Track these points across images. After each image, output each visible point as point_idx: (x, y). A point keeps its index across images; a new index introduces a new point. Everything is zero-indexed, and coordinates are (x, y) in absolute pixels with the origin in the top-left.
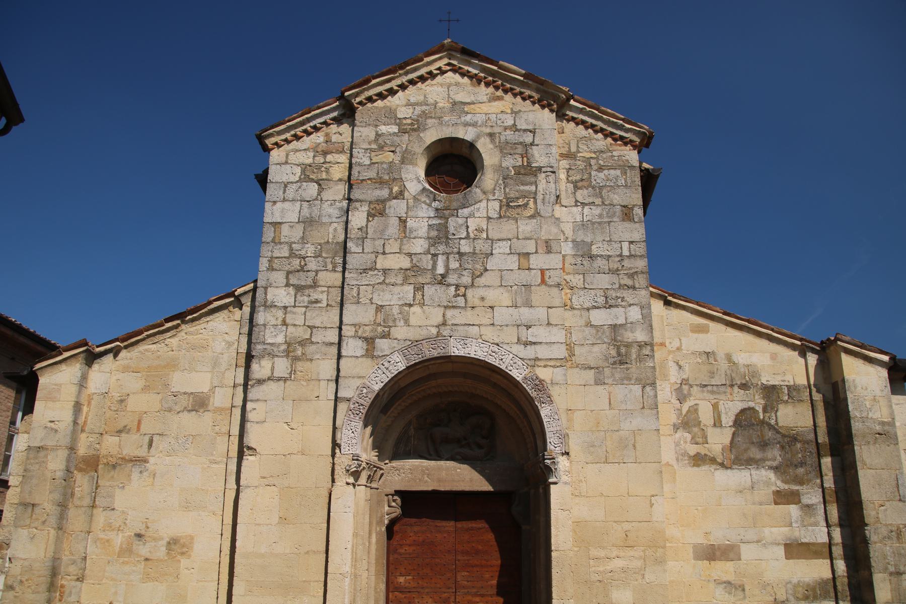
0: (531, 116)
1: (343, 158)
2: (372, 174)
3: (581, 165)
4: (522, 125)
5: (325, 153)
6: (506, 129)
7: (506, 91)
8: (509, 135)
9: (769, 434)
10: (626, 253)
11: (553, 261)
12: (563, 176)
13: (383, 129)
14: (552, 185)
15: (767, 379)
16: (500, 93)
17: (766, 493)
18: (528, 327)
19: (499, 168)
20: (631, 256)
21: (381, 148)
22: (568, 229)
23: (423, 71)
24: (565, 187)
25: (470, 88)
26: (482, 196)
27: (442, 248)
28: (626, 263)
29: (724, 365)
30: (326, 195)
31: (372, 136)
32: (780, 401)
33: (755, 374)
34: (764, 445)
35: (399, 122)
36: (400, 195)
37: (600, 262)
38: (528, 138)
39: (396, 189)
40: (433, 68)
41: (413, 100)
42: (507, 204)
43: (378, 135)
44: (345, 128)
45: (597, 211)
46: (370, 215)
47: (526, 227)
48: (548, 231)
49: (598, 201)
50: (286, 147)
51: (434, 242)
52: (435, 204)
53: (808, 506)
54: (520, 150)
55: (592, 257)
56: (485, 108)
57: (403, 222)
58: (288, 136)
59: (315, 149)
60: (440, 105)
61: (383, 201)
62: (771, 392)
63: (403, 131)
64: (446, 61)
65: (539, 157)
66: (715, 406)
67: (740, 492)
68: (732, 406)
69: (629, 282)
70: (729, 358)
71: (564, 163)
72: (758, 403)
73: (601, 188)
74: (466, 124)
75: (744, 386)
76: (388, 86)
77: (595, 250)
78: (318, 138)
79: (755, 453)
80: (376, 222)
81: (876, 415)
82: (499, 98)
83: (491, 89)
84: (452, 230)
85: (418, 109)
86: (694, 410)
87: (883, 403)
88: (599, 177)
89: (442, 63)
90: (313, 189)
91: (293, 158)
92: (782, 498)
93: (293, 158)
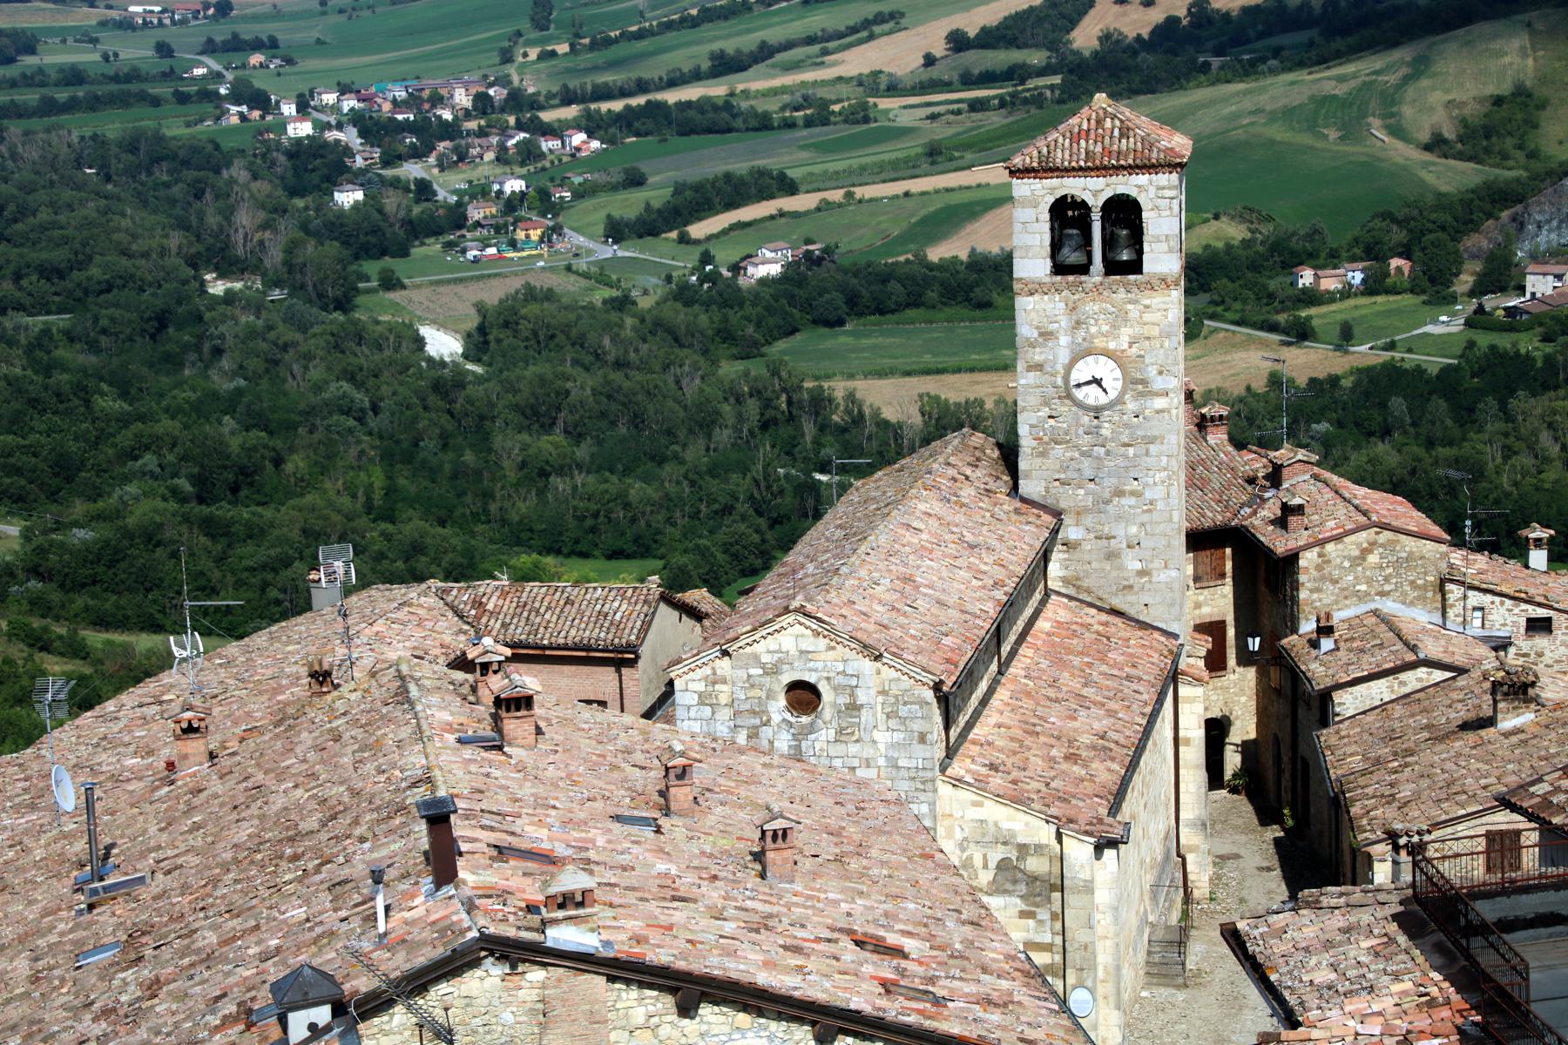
0: (856, 664)
2: (748, 707)
3: (892, 700)
4: (850, 672)
5: (714, 683)
8: (841, 680)
9: (1019, 875)
12: (879, 708)
13: (754, 671)
15: (1021, 839)
17: (1014, 911)
19: (834, 705)
21: (752, 686)
22: (882, 747)
29: (992, 828)
30: (717, 716)
32: (1027, 854)
33: (1014, 835)
34: (1015, 882)
35: (763, 666)
36: (767, 723)
37: (903, 773)
38: (854, 682)
40: (784, 624)
42: (840, 731)
43: (749, 676)
45: (902, 735)
46: (749, 737)
47: (853, 749)
48: (868, 752)
50: (686, 677)
53: (1041, 922)
55: (898, 768)
56: (823, 656)
59: (706, 678)
61: (756, 727)
62: (1023, 849)
63: (766, 673)
65: (862, 697)
66: (985, 856)
68: (996, 855)
69: (920, 786)
70: (996, 824)
71: (880, 699)
72: (1013, 855)
74: (811, 670)
75: (1005, 843)
77: (900, 763)
78: (707, 671)
79: (1009, 886)
81: (1081, 876)
82: (833, 648)
85: (776, 657)
86: (970, 858)
87: (1087, 868)
88: (903, 711)
90: (707, 711)
91: (691, 686)
92: (1024, 915)
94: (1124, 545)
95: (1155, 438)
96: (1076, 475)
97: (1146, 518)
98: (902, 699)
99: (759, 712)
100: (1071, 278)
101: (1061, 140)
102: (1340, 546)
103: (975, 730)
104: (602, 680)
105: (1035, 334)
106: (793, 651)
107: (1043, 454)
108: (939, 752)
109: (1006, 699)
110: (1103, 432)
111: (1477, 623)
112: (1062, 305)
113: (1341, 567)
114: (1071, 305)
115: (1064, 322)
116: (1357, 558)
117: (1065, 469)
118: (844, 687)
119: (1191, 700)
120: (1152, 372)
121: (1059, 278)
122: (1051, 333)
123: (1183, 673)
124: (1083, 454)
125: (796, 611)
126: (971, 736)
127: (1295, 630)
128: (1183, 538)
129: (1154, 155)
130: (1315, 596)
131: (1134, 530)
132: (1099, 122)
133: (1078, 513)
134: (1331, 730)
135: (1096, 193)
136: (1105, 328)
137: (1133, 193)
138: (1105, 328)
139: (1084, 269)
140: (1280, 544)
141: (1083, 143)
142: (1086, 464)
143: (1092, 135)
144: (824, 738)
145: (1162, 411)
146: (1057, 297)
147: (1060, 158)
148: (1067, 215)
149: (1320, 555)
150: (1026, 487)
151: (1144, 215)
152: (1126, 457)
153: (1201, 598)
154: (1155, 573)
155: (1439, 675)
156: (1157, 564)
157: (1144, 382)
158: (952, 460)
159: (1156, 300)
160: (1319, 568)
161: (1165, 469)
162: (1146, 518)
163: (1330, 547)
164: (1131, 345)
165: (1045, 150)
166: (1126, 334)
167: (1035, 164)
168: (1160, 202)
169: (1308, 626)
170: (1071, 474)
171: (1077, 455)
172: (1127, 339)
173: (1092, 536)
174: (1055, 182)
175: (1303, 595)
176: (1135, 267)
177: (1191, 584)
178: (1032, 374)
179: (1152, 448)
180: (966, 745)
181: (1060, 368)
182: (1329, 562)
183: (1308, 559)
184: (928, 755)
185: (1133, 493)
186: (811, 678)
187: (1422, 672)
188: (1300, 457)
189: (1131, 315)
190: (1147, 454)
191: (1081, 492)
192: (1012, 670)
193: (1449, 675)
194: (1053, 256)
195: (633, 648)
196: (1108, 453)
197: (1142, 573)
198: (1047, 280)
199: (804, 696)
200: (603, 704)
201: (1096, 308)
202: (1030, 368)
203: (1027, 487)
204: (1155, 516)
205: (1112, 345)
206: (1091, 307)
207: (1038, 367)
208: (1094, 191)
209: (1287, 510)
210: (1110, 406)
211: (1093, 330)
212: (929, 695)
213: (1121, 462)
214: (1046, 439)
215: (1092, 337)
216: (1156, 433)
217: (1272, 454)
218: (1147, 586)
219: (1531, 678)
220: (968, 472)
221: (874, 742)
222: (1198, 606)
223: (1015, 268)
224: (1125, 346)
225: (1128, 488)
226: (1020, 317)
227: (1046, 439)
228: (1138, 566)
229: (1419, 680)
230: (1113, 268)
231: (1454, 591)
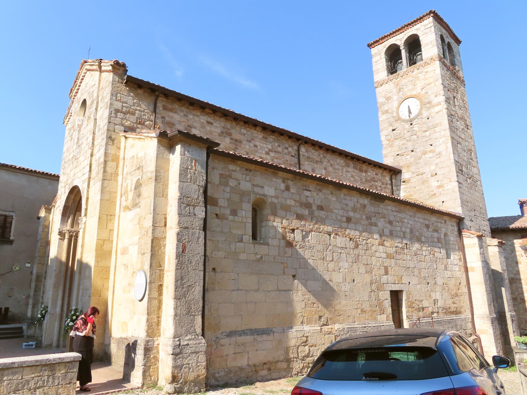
18: (85, 168)
23: (81, 77)
40: (83, 74)
67: (132, 221)
89: (84, 71)
94: (429, 176)
95: (437, 124)
97: (438, 161)
105: (384, 99)
107: (391, 146)
110: (415, 129)
112: (393, 85)
114: (396, 83)
115: (395, 91)
117: (400, 149)
120: (432, 97)
122: (390, 97)
124: (407, 141)
131: (433, 167)
133: (408, 166)
136: (411, 87)
137: (415, 32)
138: (411, 87)
145: (439, 112)
146: (391, 83)
151: (420, 38)
152: (426, 136)
157: (429, 102)
159: (429, 68)
161: (444, 136)
162: (438, 161)
166: (419, 85)
170: (403, 151)
171: (405, 142)
172: (420, 88)
173: (415, 175)
178: (384, 116)
179: (436, 129)
181: (394, 109)
185: (430, 152)
191: (408, 157)
197: (439, 187)
198: (387, 77)
205: (414, 93)
206: (404, 81)
207: (387, 112)
208: (400, 40)
210: (416, 117)
211: (406, 90)
213: (425, 139)
218: (443, 193)
223: (375, 79)
224: (420, 91)
225: (428, 150)
226: (378, 95)
227: (392, 139)
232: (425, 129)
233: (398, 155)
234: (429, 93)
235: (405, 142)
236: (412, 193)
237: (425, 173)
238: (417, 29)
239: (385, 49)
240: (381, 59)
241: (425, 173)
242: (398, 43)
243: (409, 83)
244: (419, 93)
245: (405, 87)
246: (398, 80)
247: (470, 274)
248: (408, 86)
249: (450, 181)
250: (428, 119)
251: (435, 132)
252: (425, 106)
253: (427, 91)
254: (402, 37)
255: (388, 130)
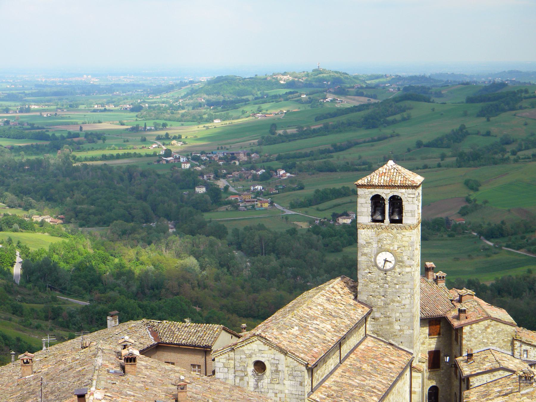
1: (233, 362)
3: (291, 369)
5: (229, 360)
6: (272, 359)
7: (272, 348)
8: (273, 361)
10: (300, 394)
11: (282, 395)
12: (286, 372)
14: (283, 375)
16: (270, 348)
20: (301, 395)
24: (287, 375)
25: (263, 346)
26: (266, 377)
27: (257, 390)
28: (300, 397)
30: (229, 372)
31: (239, 358)
38: (278, 363)
39: (246, 374)
40: (254, 340)
41: (249, 349)
42: (272, 379)
43: (241, 358)
44: (232, 353)
45: (294, 382)
47: (276, 386)
49: (294, 380)
51: (255, 388)
52: (255, 378)
54: (275, 365)
56: (267, 352)
57: (248, 383)
58: (219, 354)
59: (226, 358)
60: (256, 350)
61: (243, 377)
63: (247, 357)
64: (256, 338)
65: (280, 368)
71: (287, 369)
73: (295, 376)
74: (262, 357)
76: (242, 344)
78: (226, 355)
80: (241, 382)
82: (270, 350)
83: (268, 347)
84: (259, 385)
85: (251, 351)
90: (226, 370)
91: (221, 360)
93: (221, 360)
94: (394, 320)
95: (406, 282)
96: (378, 294)
97: (402, 311)
98: (294, 369)
99: (244, 370)
100: (377, 224)
101: (375, 175)
102: (477, 325)
103: (325, 383)
104: (199, 359)
105: (365, 243)
106: (257, 350)
107: (366, 286)
108: (308, 389)
109: (340, 372)
110: (387, 279)
111: (525, 356)
112: (374, 233)
113: (478, 333)
114: (377, 233)
116: (483, 330)
118: (274, 364)
119: (416, 377)
120: (405, 258)
121: (373, 223)
122: (370, 243)
123: (414, 368)
125: (258, 335)
126: (323, 384)
127: (461, 355)
128: (419, 319)
129: (407, 182)
130: (468, 343)
131: (398, 315)
132: (389, 170)
134: (468, 391)
135: (386, 194)
136: (389, 242)
137: (400, 195)
139: (382, 221)
140: (456, 324)
141: (383, 177)
142: (381, 290)
143: (386, 174)
144: (266, 382)
146: (373, 231)
147: (375, 182)
148: (377, 201)
149: (471, 328)
150: (359, 297)
151: (403, 203)
153: (431, 342)
154: (405, 331)
155: (507, 374)
156: (406, 327)
157: (402, 262)
158: (336, 286)
159: (407, 233)
160: (470, 333)
162: (402, 311)
163: (474, 325)
164: (398, 248)
165: (369, 179)
167: (366, 183)
168: (409, 199)
169: (465, 354)
171: (378, 287)
174: (372, 190)
175: (464, 342)
176: (400, 221)
177: (428, 336)
179: (405, 286)
180: (321, 387)
182: (473, 331)
183: (466, 329)
184: (303, 390)
186: (263, 360)
187: (501, 372)
188: (468, 293)
189: (398, 238)
190: (403, 288)
191: (380, 300)
192: (345, 362)
193: (510, 373)
194: (372, 216)
195: (210, 347)
196: (389, 287)
197: (400, 330)
199: (260, 366)
200: (199, 366)
201: (386, 235)
202: (362, 255)
203: (362, 297)
204: (405, 310)
205: (391, 248)
206: (384, 234)
208: (386, 194)
209: (460, 311)
210: (390, 270)
212: (304, 368)
214: (367, 280)
215: (385, 245)
216: (406, 280)
217: (459, 291)
219: (532, 375)
220: (340, 290)
221: (284, 384)
222: (430, 344)
224: (396, 249)
226: (359, 236)
228: (399, 328)
229: (500, 375)
230: (392, 221)
231: (517, 344)
232: (396, 282)
233: (371, 295)
234: (404, 254)
235: (378, 287)
236: (379, 330)
237: (391, 317)
238: (401, 193)
239: (371, 196)
240: (366, 203)
241: (391, 317)
242: (383, 196)
243: (388, 238)
244: (395, 251)
245: (385, 239)
246: (379, 230)
247: (412, 395)
248: (388, 240)
249: (409, 329)
250: (400, 274)
251: (403, 288)
252: (399, 263)
253: (402, 251)
254: (388, 193)
255: (366, 271)
